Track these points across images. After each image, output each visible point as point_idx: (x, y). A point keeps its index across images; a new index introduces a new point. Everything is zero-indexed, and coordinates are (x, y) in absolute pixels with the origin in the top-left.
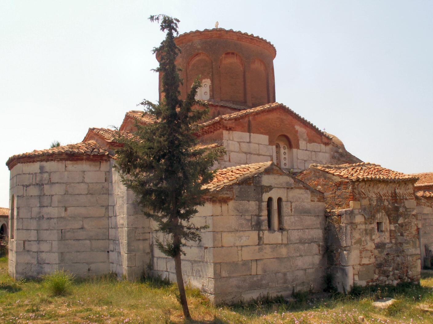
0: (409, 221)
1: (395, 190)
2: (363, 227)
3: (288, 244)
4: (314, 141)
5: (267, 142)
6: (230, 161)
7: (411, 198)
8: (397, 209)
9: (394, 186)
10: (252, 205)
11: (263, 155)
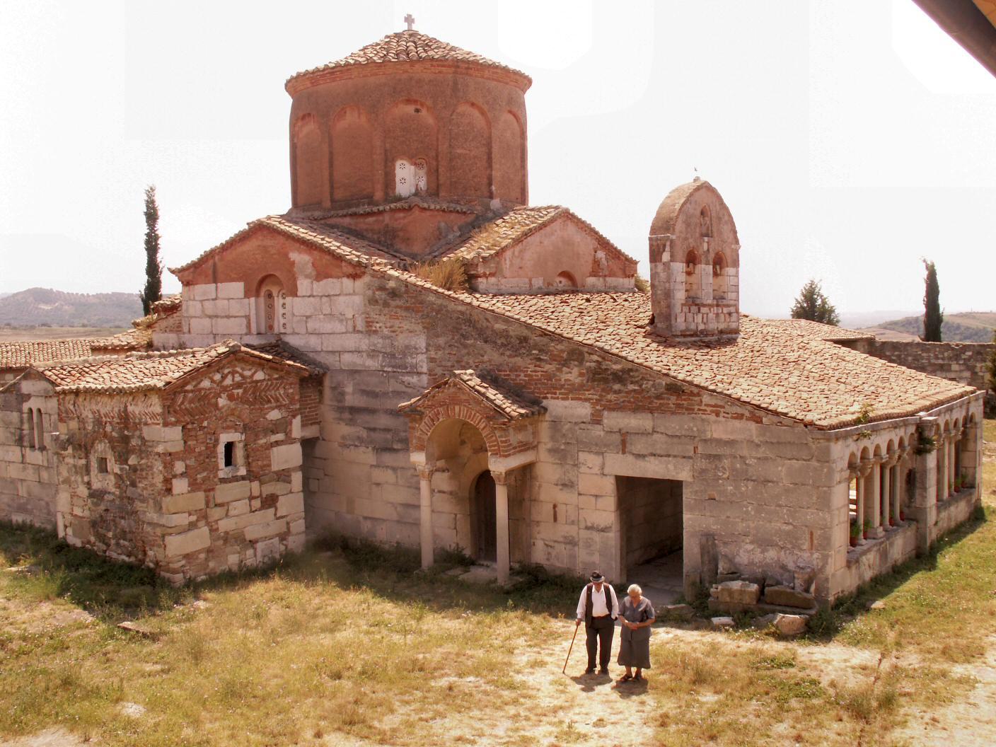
0: (149, 464)
1: (126, 407)
2: (71, 461)
3: (48, 467)
4: (328, 276)
5: (241, 295)
6: (189, 331)
7: (156, 421)
8: (125, 440)
9: (124, 399)
10: (14, 416)
11: (235, 317)
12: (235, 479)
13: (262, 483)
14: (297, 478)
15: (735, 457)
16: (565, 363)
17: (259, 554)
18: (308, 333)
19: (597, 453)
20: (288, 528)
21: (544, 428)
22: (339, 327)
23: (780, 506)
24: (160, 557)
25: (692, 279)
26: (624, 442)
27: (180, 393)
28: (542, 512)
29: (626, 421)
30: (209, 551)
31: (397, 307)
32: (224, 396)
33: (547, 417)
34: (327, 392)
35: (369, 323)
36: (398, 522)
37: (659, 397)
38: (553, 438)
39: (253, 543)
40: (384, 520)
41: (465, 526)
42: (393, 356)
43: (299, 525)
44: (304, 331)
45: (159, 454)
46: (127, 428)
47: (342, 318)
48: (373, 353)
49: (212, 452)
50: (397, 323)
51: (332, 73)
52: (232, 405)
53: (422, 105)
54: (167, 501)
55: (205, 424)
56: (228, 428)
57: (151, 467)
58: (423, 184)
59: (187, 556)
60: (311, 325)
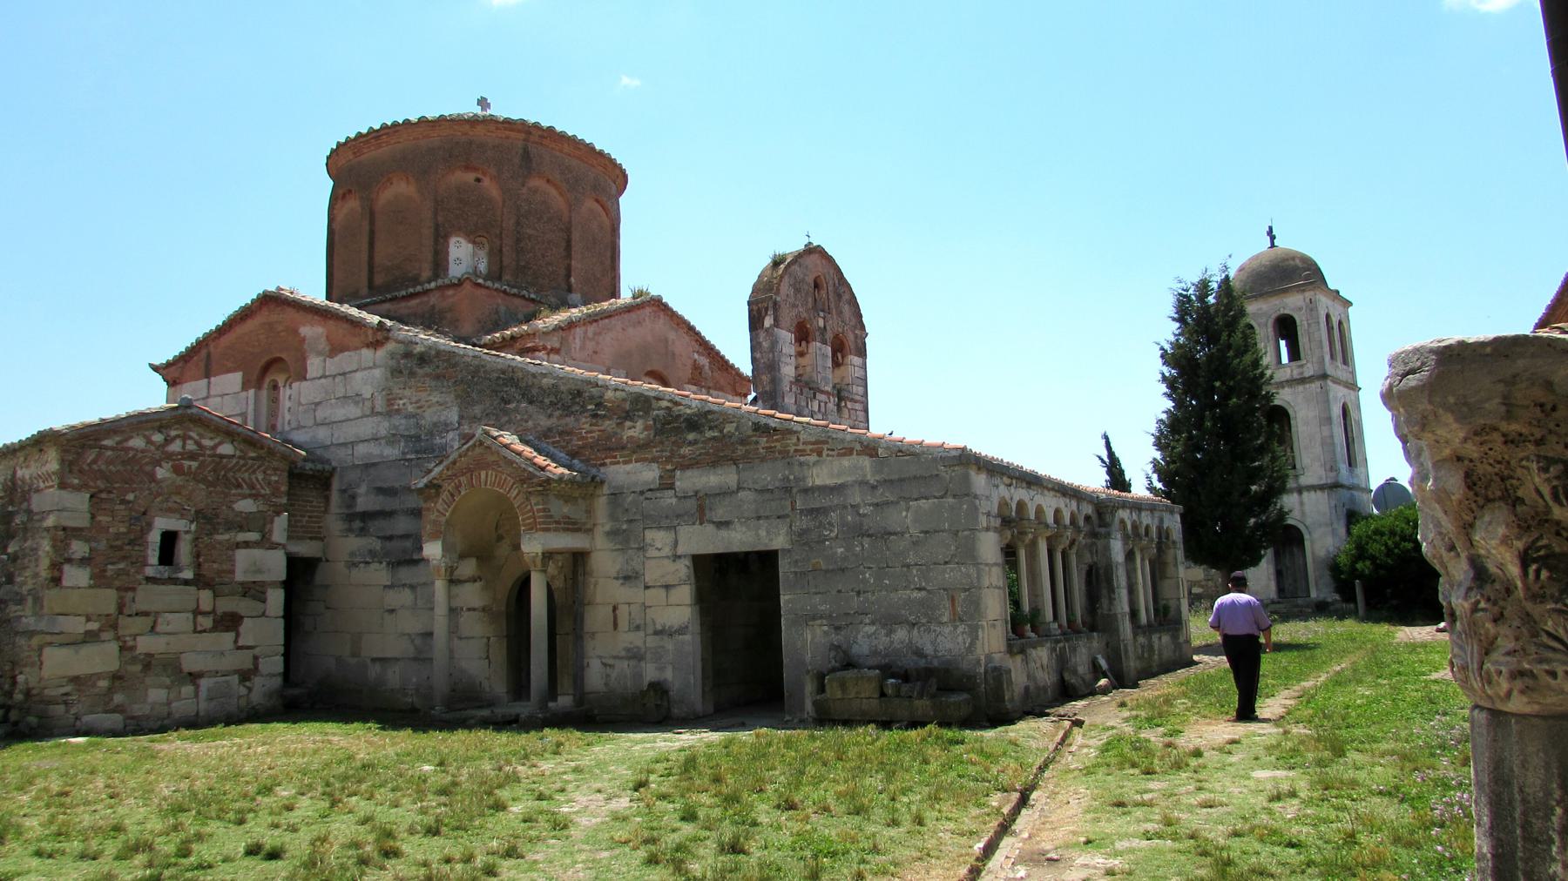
5: (238, 387)
12: (173, 581)
13: (215, 596)
14: (276, 598)
15: (845, 507)
16: (629, 416)
17: (203, 693)
18: (317, 425)
19: (668, 528)
20: (256, 668)
21: (601, 504)
22: (353, 411)
23: (908, 566)
24: (33, 683)
25: (803, 361)
26: (701, 508)
27: (91, 447)
28: (596, 618)
29: (704, 479)
30: (116, 677)
31: (427, 375)
32: (168, 465)
33: (606, 490)
34: (335, 497)
35: (390, 402)
36: (415, 659)
37: (743, 442)
38: (613, 517)
39: (194, 677)
40: (397, 659)
41: (500, 653)
42: (418, 438)
43: (275, 664)
44: (311, 423)
45: (47, 530)
46: (11, 502)
47: (357, 398)
48: (392, 439)
49: (139, 540)
50: (423, 395)
51: (377, 138)
52: (179, 480)
53: (484, 174)
54: (51, 596)
55: (130, 497)
56: (170, 510)
57: (35, 550)
58: (483, 267)
59: (75, 680)
60: (321, 414)
